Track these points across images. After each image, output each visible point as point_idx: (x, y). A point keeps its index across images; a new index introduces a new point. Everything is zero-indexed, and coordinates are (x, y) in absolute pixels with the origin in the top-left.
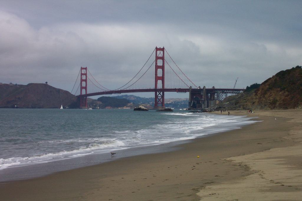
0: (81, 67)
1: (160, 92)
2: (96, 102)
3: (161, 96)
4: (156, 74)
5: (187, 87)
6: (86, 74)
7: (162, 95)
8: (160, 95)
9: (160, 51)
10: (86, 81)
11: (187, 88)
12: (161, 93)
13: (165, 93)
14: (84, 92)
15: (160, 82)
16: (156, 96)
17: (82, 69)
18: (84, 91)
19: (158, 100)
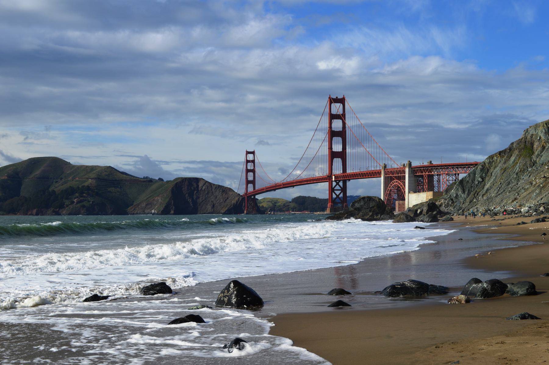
0: (246, 151)
1: (338, 181)
2: (290, 204)
3: (340, 189)
4: (330, 148)
5: (378, 165)
6: (253, 161)
7: (342, 186)
8: (338, 187)
9: (339, 104)
10: (253, 171)
11: (379, 167)
12: (341, 184)
13: (349, 184)
14: (251, 188)
15: (337, 162)
16: (332, 190)
17: (248, 153)
18: (250, 186)
19: (334, 196)
